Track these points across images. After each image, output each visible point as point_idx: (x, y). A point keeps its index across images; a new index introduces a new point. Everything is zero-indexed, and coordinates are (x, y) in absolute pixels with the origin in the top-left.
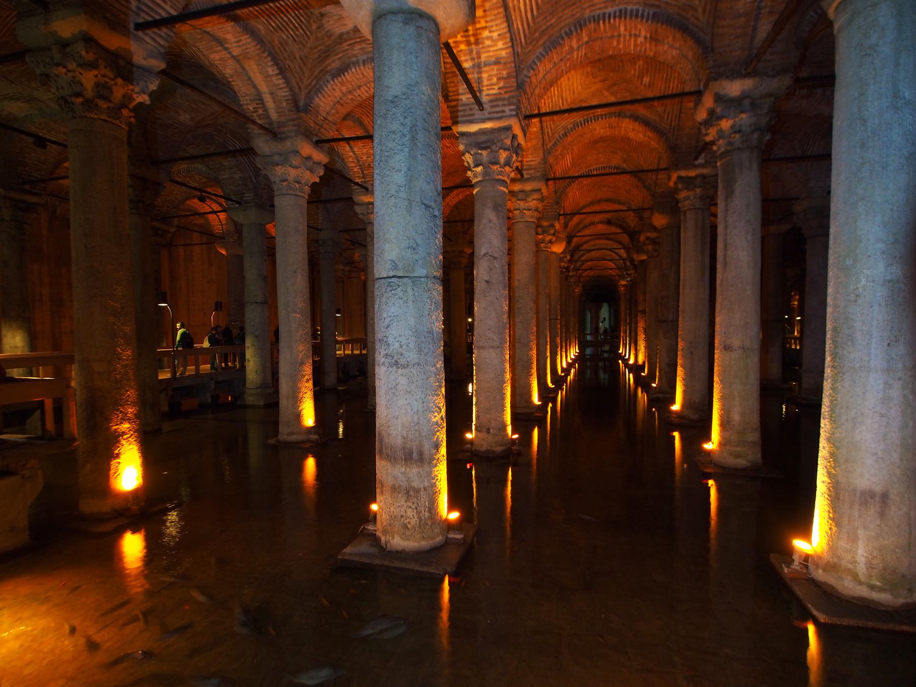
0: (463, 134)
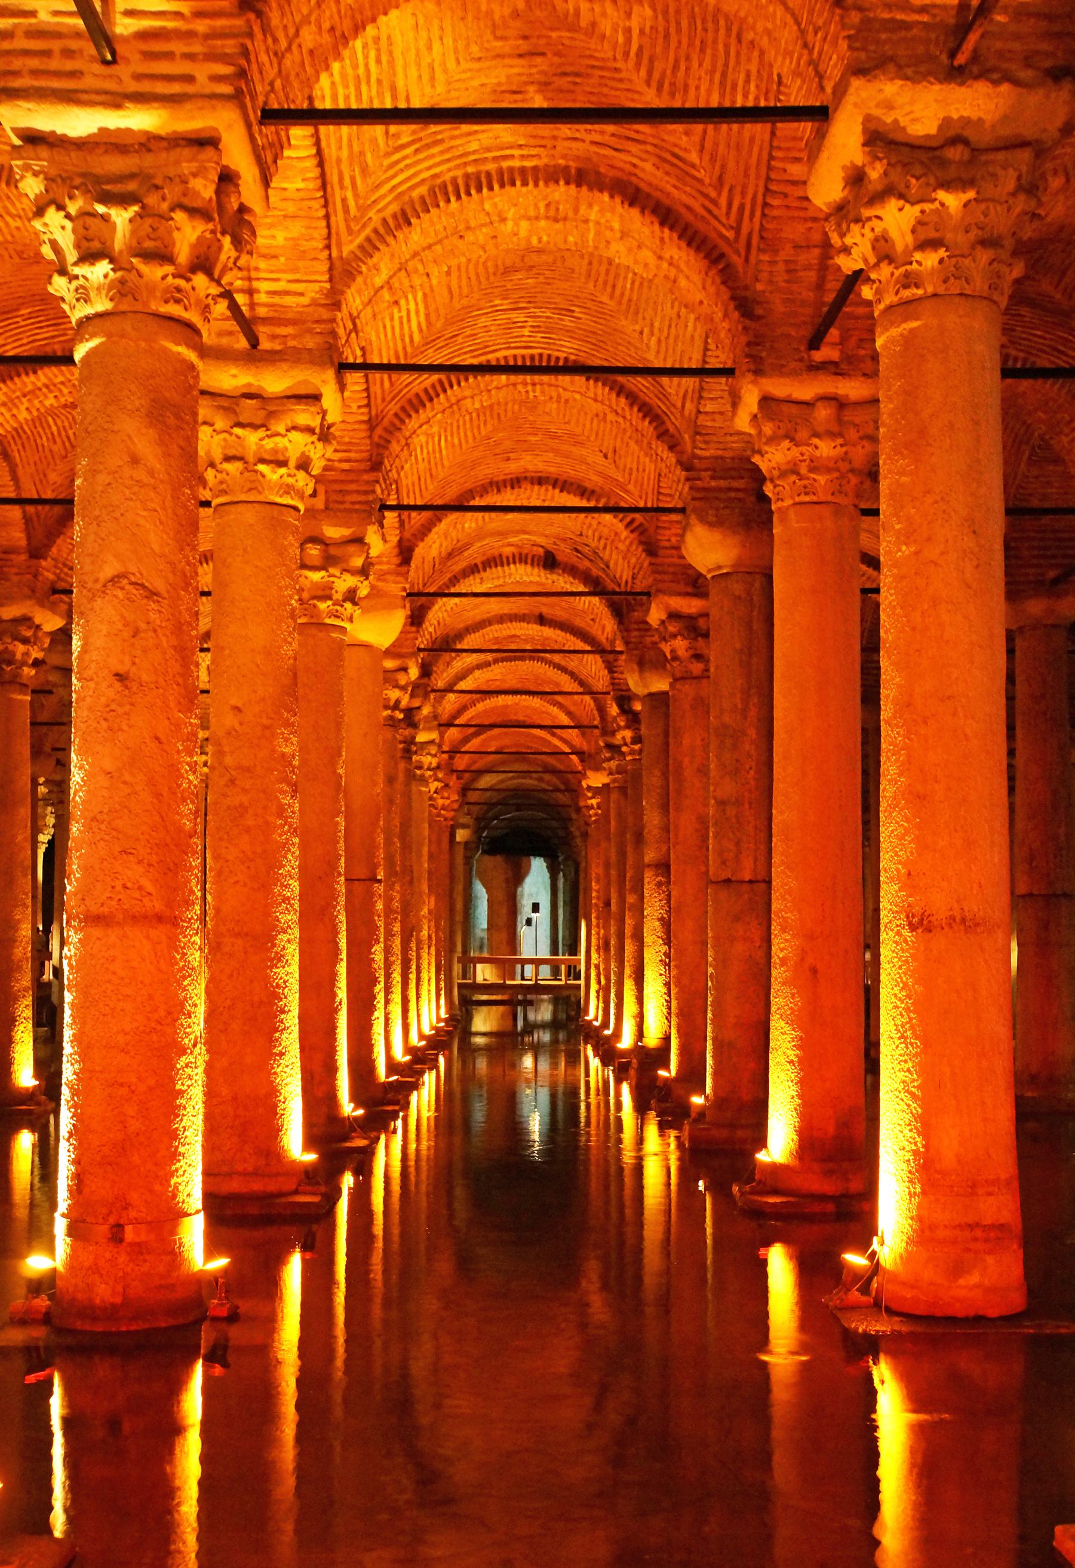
0: (33, 139)
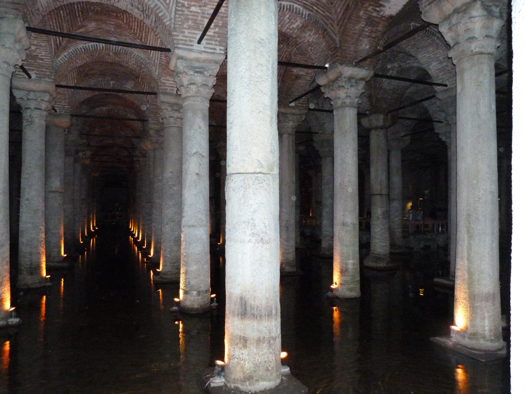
0: (181, 58)
